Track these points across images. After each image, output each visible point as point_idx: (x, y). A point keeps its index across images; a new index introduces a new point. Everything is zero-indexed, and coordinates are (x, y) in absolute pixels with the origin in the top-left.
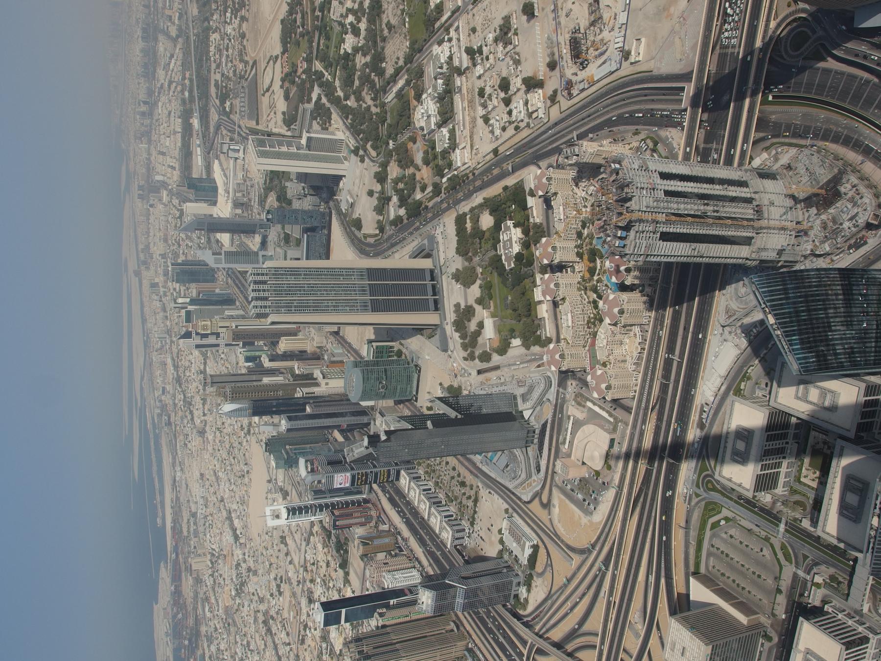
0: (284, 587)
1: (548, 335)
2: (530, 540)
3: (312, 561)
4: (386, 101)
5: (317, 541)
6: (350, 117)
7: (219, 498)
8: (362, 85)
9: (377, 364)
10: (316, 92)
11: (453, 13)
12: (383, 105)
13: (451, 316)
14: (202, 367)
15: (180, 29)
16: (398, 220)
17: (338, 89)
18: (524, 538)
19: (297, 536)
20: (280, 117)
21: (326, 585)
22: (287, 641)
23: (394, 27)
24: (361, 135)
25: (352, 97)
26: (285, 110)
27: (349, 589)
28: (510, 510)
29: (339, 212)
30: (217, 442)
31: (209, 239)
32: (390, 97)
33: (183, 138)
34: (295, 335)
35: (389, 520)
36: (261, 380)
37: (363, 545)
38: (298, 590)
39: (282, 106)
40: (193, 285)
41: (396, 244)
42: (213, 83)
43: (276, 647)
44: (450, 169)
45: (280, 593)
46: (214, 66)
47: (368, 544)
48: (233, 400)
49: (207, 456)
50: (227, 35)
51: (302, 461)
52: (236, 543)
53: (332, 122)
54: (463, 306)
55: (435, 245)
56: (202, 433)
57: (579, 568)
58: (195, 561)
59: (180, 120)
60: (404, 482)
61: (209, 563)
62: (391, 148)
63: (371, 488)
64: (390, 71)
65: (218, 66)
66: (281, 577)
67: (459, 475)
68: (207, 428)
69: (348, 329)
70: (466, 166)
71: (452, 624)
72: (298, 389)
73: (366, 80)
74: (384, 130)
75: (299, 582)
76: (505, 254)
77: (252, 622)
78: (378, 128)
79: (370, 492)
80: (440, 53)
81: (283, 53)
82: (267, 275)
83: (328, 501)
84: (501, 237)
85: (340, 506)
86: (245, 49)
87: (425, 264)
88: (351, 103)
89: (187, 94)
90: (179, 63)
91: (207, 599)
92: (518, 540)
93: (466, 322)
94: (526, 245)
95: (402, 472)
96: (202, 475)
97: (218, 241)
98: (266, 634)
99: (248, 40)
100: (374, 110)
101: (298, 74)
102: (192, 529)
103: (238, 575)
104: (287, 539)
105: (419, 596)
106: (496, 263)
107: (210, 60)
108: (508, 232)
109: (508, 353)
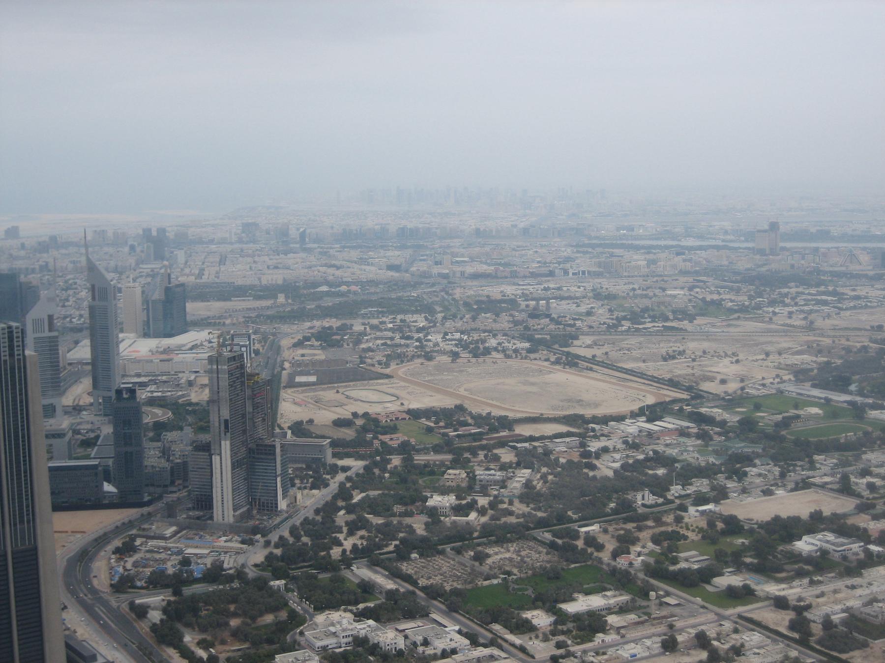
4: (354, 568)
8: (379, 529)
10: (356, 465)
11: (522, 649)
12: (346, 561)
15: (425, 275)
16: (141, 612)
17: (363, 494)
23: (481, 564)
25: (352, 517)
26: (316, 422)
31: (80, 330)
32: (362, 572)
33: (252, 287)
39: (324, 417)
41: (95, 617)
42: (348, 322)
46: (375, 322)
50: (425, 336)
53: (306, 491)
59: (280, 282)
62: (272, 583)
64: (406, 568)
65: (373, 327)
73: (387, 532)
78: (304, 561)
80: (449, 636)
81: (409, 412)
82: (12, 355)
86: (408, 361)
88: (341, 517)
89: (324, 288)
90: (371, 276)
97: (77, 343)
99: (422, 364)
100: (336, 553)
101: (380, 437)
107: (383, 316)
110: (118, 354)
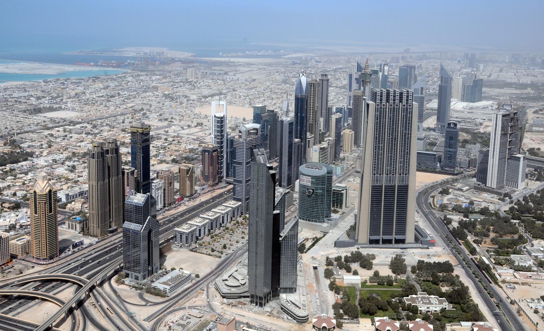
0: (166, 123)
1: (344, 325)
2: (172, 289)
3: (180, 141)
5: (196, 146)
6: (539, 195)
7: (236, 89)
9: (329, 189)
13: (365, 252)
14: (334, 85)
16: (449, 221)
18: (173, 285)
19: (201, 134)
20: (536, 147)
21: (162, 148)
22: (125, 122)
24: (523, 202)
27: (156, 162)
28: (198, 279)
29: (456, 180)
30: (277, 91)
33: (515, 84)
34: (355, 144)
35: (204, 194)
36: (321, 116)
37: (187, 170)
38: (162, 131)
40: (397, 80)
43: (122, 114)
44: (495, 264)
45: (161, 120)
47: (188, 174)
48: (310, 85)
49: (268, 83)
51: (258, 126)
52: (203, 96)
53: (533, 182)
54: (374, 262)
55: (426, 246)
56: (285, 82)
57: (140, 326)
58: (194, 71)
59: (529, 83)
60: (232, 203)
61: (191, 80)
63: (230, 183)
66: (173, 122)
67: (231, 245)
68: (288, 85)
69: (358, 180)
70: (498, 276)
71: (115, 228)
72: (313, 135)
74: (527, 217)
75: (167, 132)
76: (417, 298)
77: (144, 102)
78: (529, 214)
79: (227, 183)
83: (225, 149)
84: (432, 296)
85: (220, 158)
87: (410, 236)
91: (165, 77)
92: (172, 280)
93: (359, 263)
94: (426, 318)
95: (240, 203)
96: (254, 80)
97: (431, 100)
98: (134, 110)
102: (216, 72)
103: (179, 96)
104: (200, 127)
105: (142, 195)
106: (410, 290)
108: (437, 302)
109: (330, 292)
110: (450, 107)
